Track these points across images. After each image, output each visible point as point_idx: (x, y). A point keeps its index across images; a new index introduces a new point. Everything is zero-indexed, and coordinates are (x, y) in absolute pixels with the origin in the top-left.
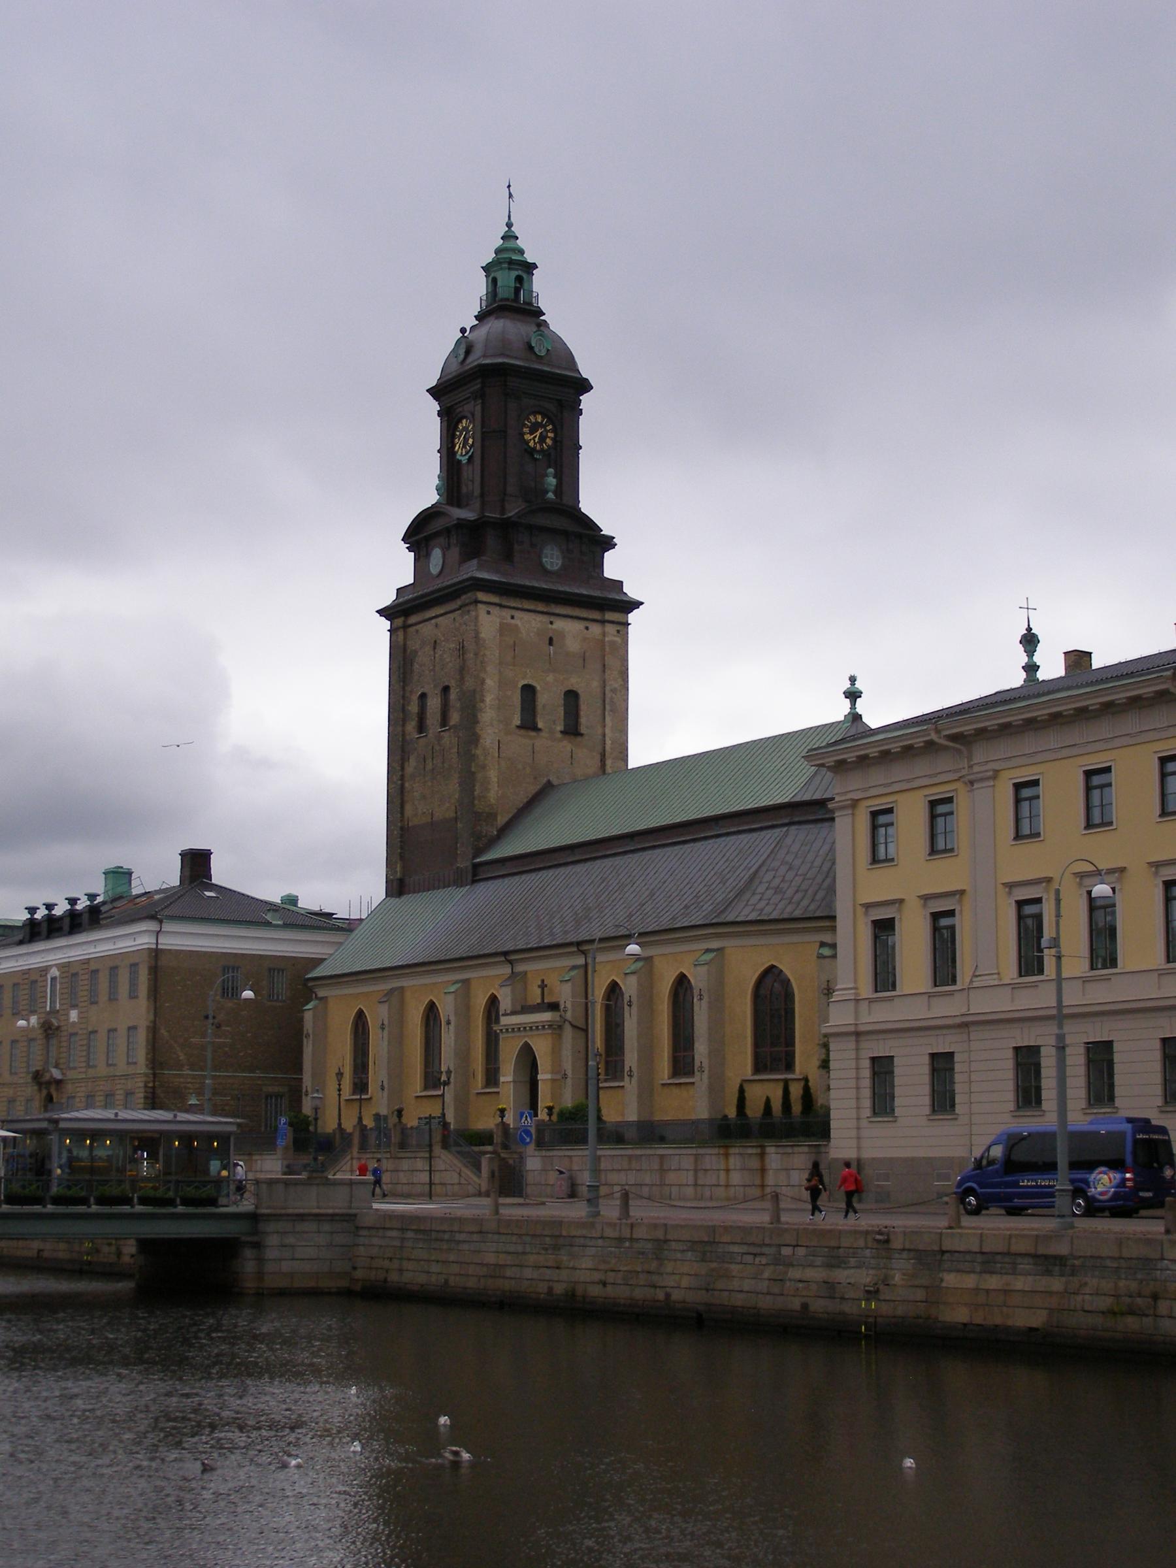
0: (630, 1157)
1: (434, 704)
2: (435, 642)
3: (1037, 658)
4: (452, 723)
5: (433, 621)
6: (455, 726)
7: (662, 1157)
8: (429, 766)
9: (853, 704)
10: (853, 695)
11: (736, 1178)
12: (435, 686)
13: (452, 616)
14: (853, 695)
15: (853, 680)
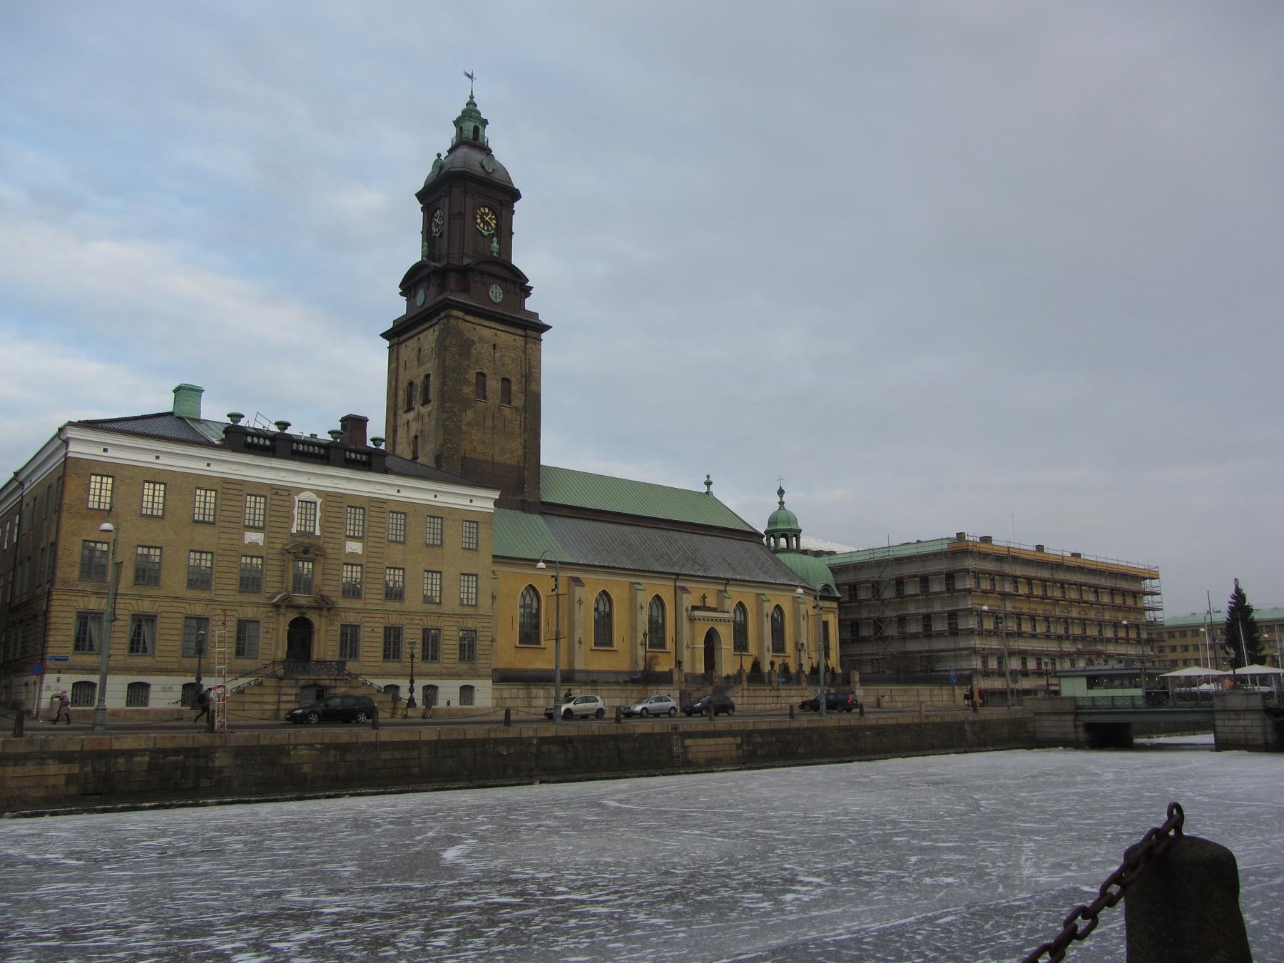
0: (904, 690)
1: (493, 384)
2: (494, 345)
3: (784, 499)
4: (514, 404)
5: (493, 331)
6: (516, 408)
7: (917, 690)
8: (489, 423)
9: (708, 487)
10: (708, 484)
11: (945, 698)
12: (495, 374)
13: (513, 337)
14: (708, 484)
15: (708, 477)
